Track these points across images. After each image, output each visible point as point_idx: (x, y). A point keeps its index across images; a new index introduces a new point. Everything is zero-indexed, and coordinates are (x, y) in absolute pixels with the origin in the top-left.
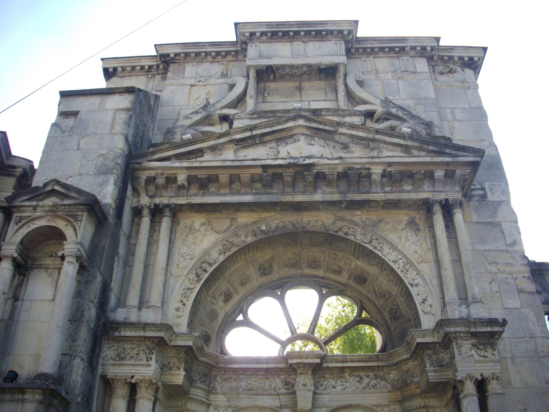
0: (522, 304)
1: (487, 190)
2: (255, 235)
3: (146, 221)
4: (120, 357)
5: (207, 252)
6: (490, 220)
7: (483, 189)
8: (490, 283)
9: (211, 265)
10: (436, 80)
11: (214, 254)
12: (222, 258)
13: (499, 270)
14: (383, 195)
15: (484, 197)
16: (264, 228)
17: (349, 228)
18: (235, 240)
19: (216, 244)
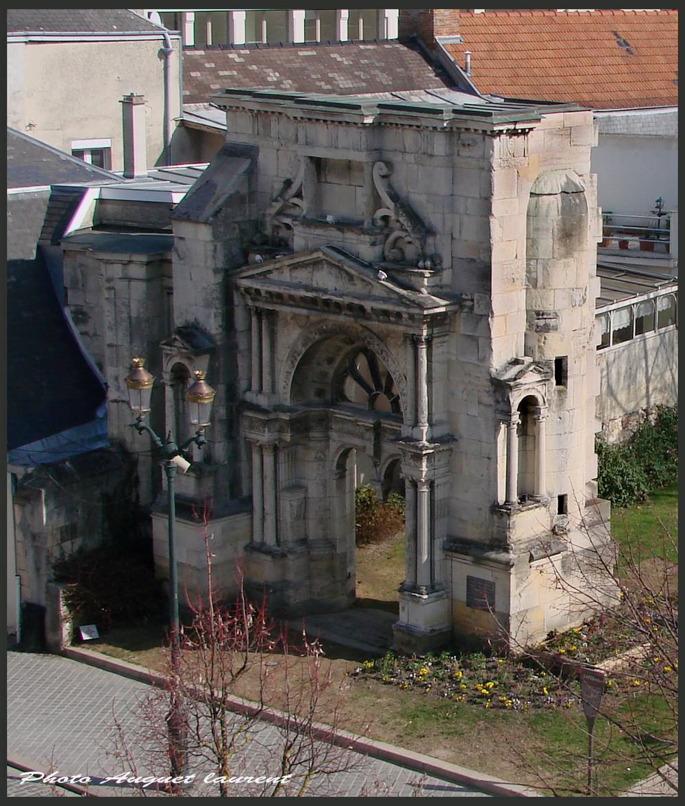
0: (479, 414)
1: (475, 301)
2: (320, 334)
3: (254, 319)
4: (251, 428)
5: (295, 344)
6: (471, 334)
7: (472, 300)
8: (463, 392)
9: (299, 355)
10: (458, 155)
11: (300, 344)
12: (304, 350)
13: (470, 381)
14: (377, 323)
15: (472, 308)
16: (324, 327)
17: (371, 338)
18: (310, 336)
19: (298, 338)
